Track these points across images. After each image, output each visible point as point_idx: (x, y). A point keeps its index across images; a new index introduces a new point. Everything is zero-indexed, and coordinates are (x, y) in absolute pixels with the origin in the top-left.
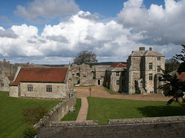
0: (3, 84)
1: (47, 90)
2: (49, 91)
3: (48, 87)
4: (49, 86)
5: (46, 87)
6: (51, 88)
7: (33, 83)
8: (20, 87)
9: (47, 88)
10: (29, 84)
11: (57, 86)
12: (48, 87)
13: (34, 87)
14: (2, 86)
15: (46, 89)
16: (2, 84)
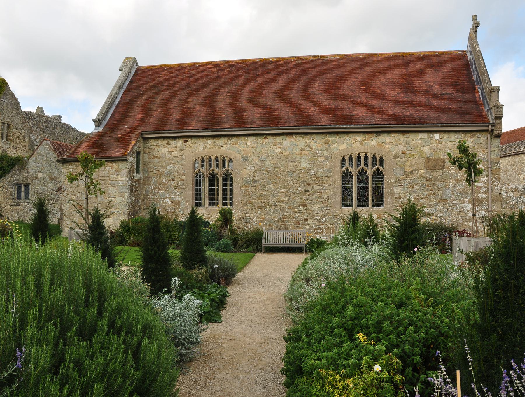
0: (27, 186)
1: (346, 190)
2: (362, 202)
3: (354, 171)
4: (362, 159)
5: (338, 164)
6: (379, 177)
7: (241, 142)
8: (138, 172)
9: (346, 176)
10: (204, 147)
11: (428, 160)
12: (354, 171)
13: (242, 174)
14: (19, 196)
15: (339, 181)
16: (19, 185)
